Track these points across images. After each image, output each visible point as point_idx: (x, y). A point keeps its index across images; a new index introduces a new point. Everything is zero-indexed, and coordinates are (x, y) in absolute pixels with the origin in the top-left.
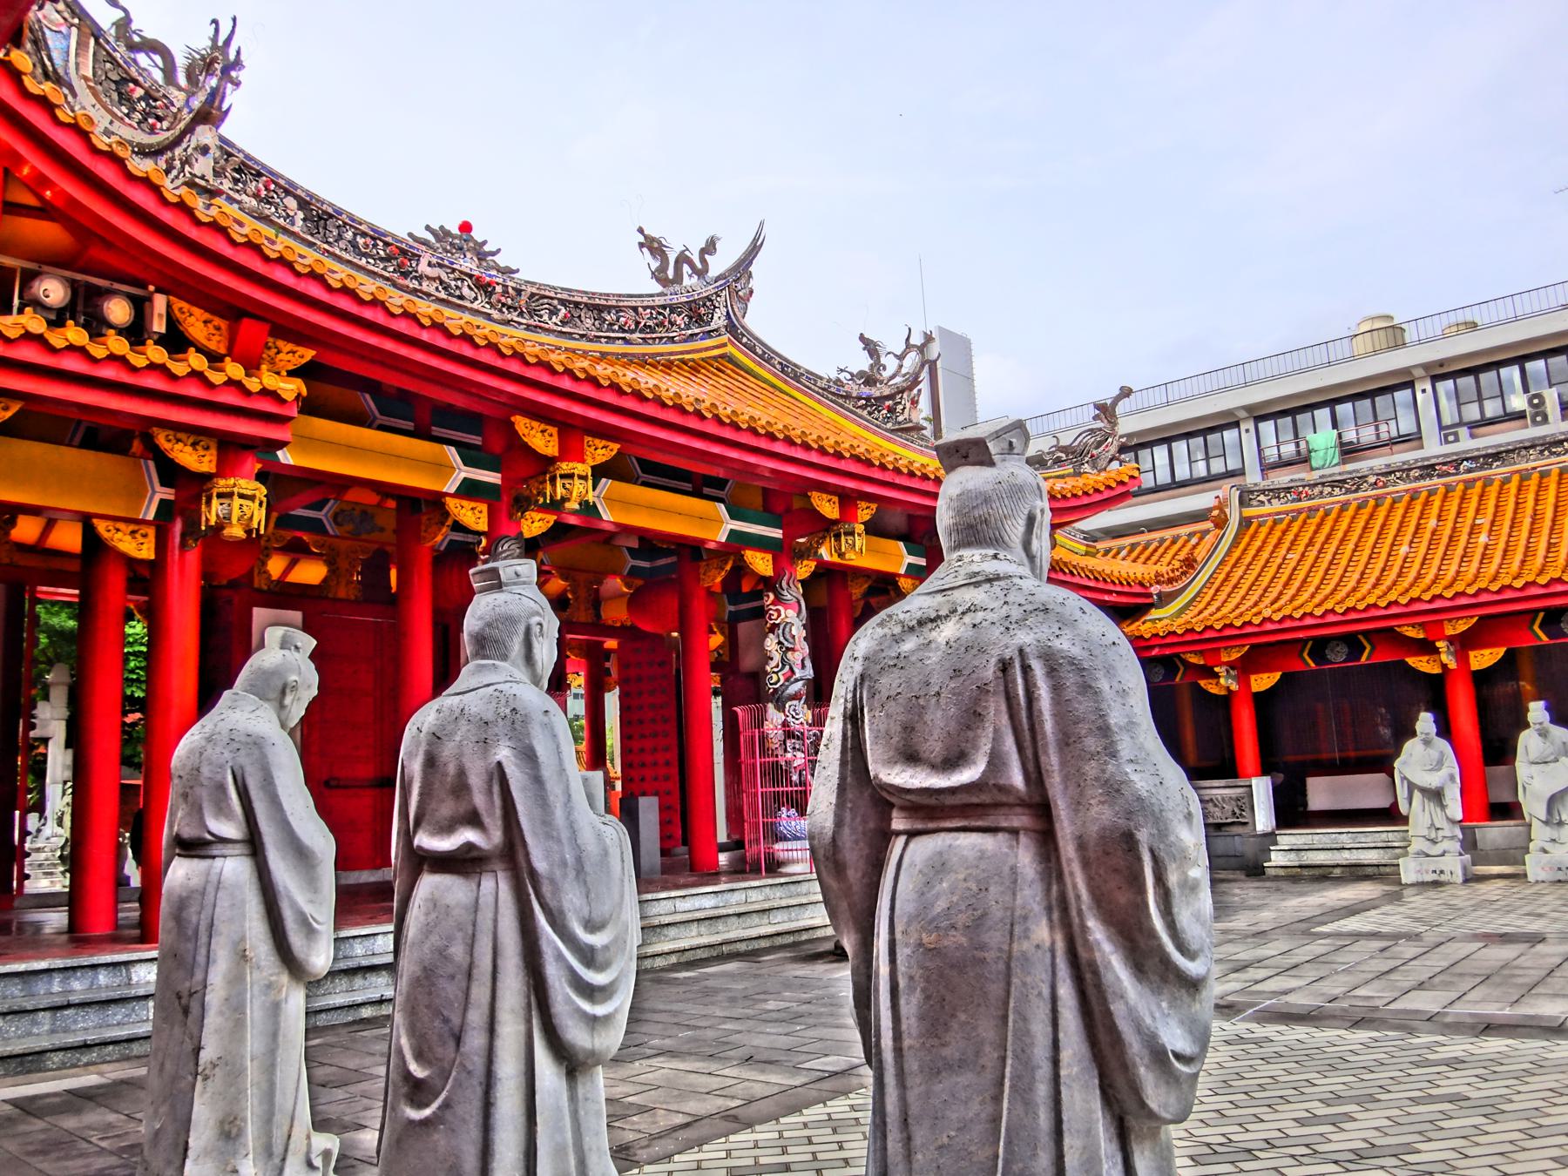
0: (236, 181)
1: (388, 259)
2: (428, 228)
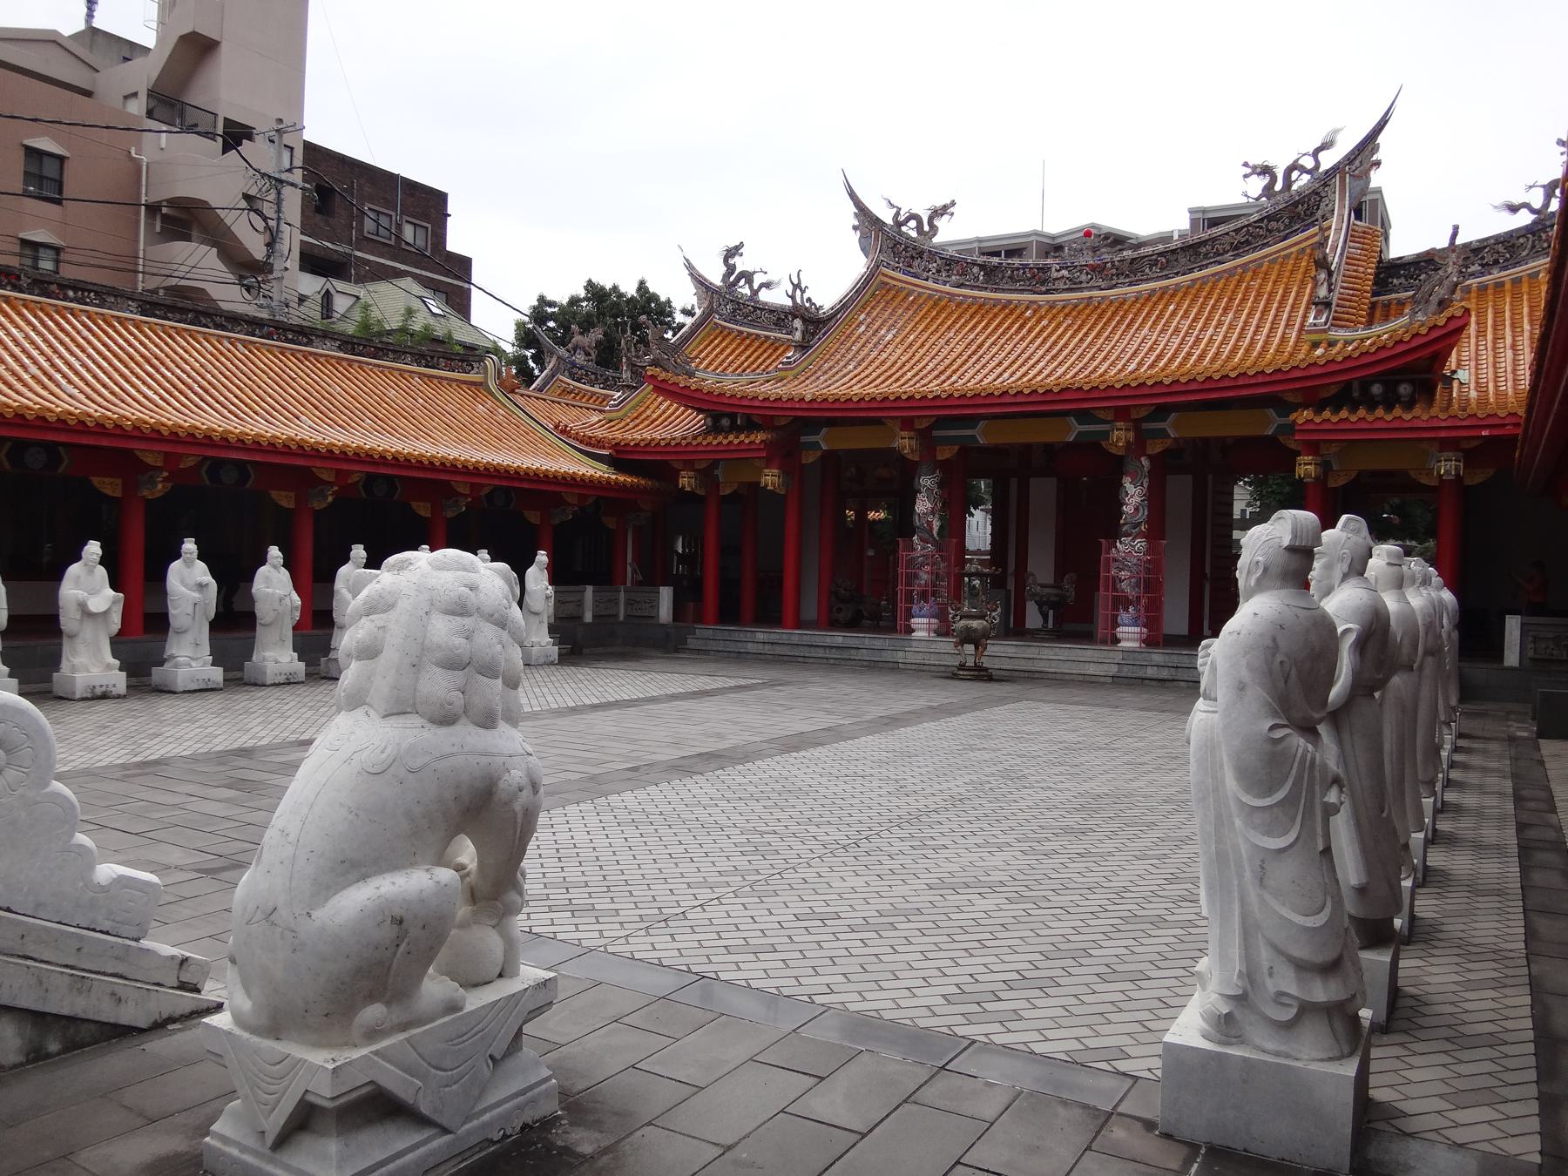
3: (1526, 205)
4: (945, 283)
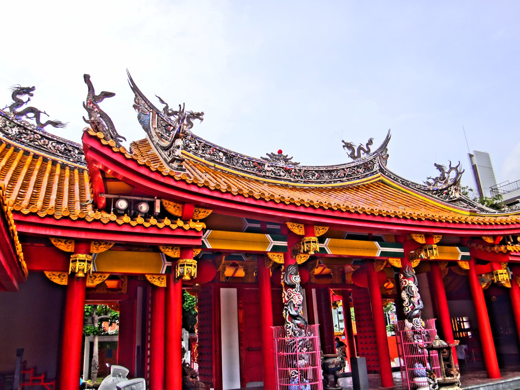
0: (203, 150)
1: (254, 167)
2: (267, 154)
4: (202, 157)
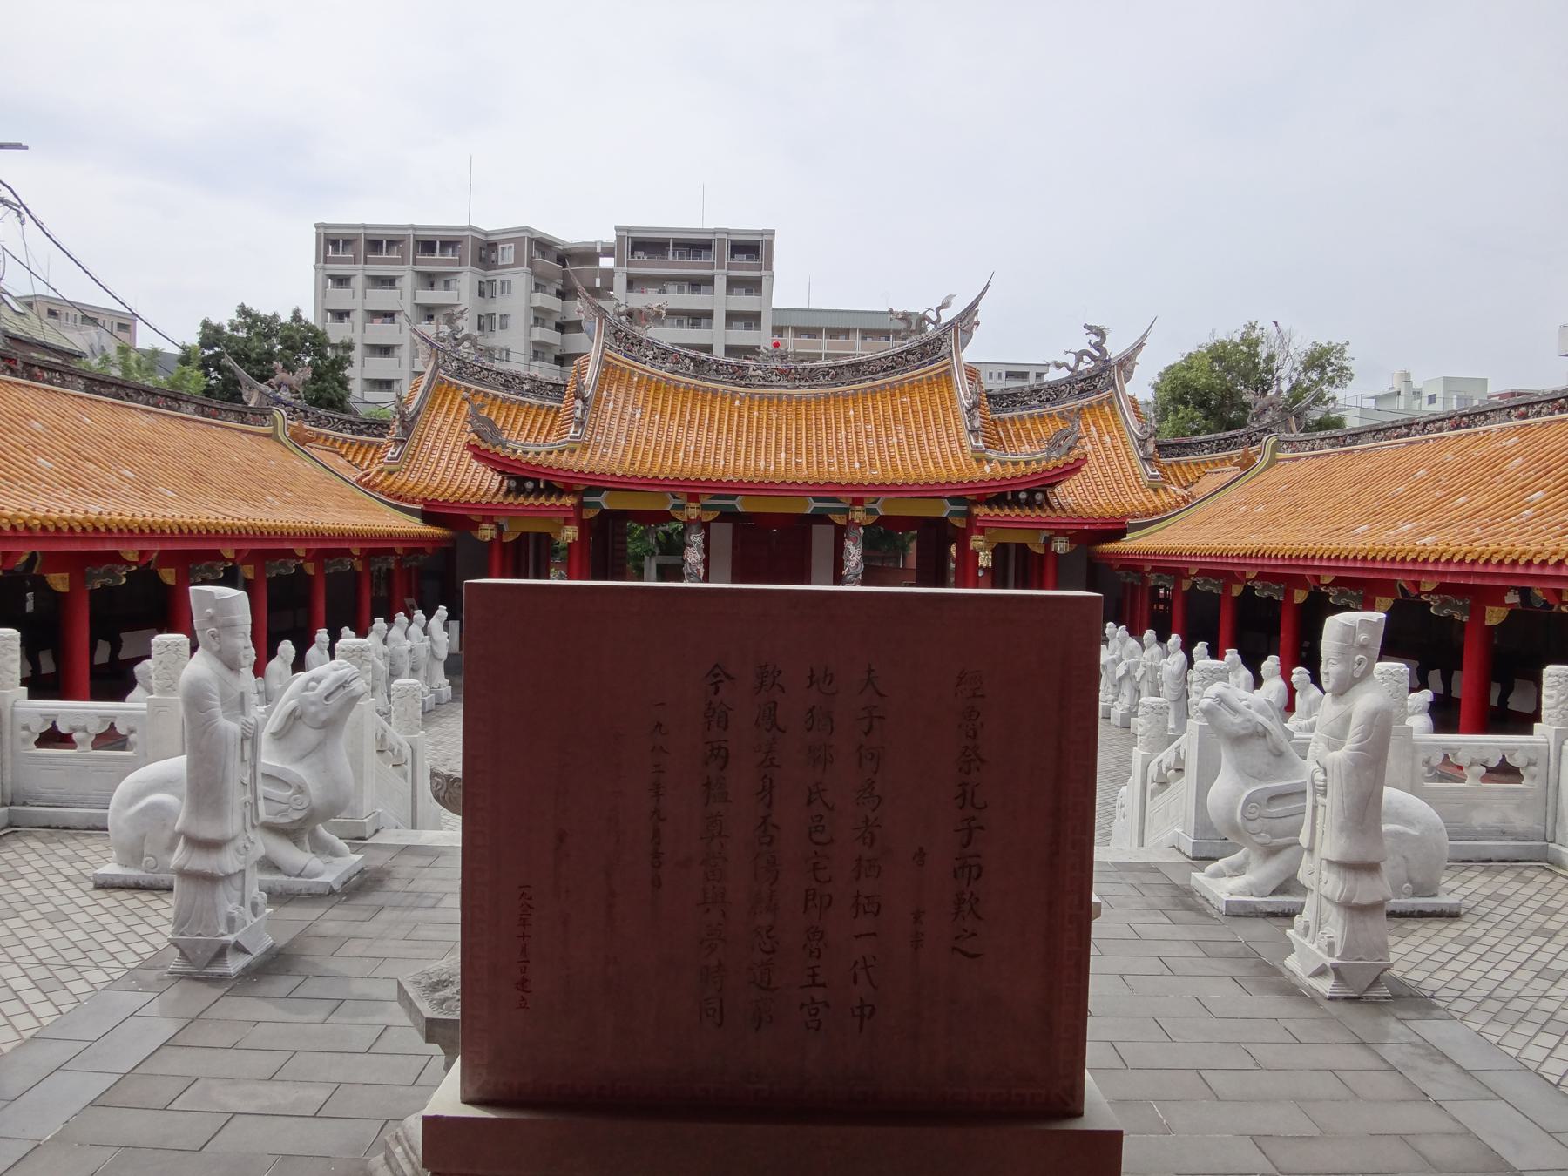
3: (1066, 365)
